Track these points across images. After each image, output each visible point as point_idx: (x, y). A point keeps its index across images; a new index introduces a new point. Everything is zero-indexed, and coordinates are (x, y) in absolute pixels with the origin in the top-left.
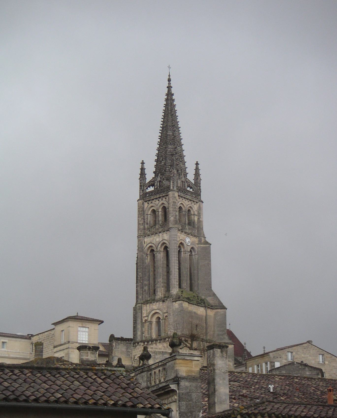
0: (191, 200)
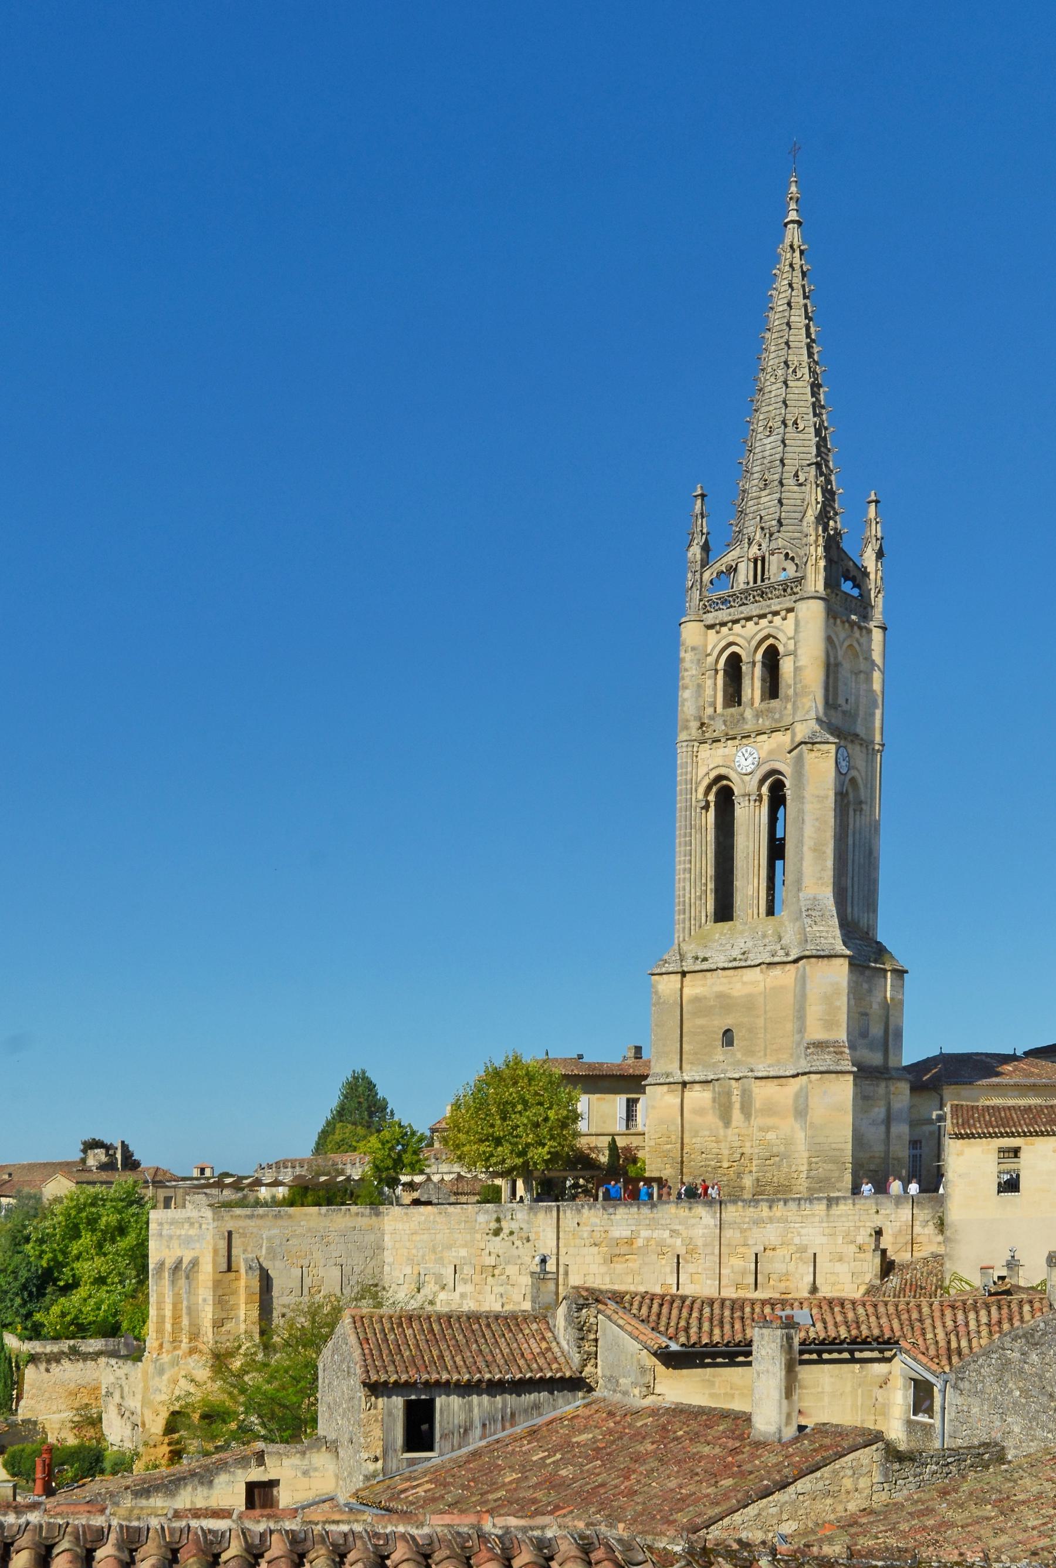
0: (762, 616)
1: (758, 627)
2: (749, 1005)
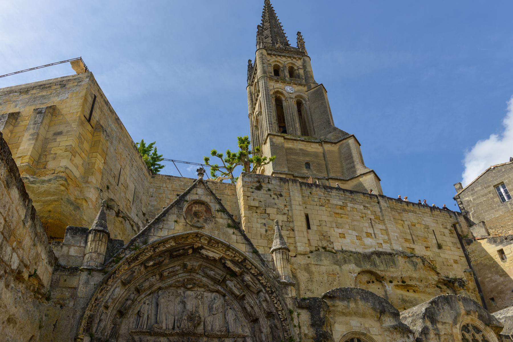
2: (316, 155)
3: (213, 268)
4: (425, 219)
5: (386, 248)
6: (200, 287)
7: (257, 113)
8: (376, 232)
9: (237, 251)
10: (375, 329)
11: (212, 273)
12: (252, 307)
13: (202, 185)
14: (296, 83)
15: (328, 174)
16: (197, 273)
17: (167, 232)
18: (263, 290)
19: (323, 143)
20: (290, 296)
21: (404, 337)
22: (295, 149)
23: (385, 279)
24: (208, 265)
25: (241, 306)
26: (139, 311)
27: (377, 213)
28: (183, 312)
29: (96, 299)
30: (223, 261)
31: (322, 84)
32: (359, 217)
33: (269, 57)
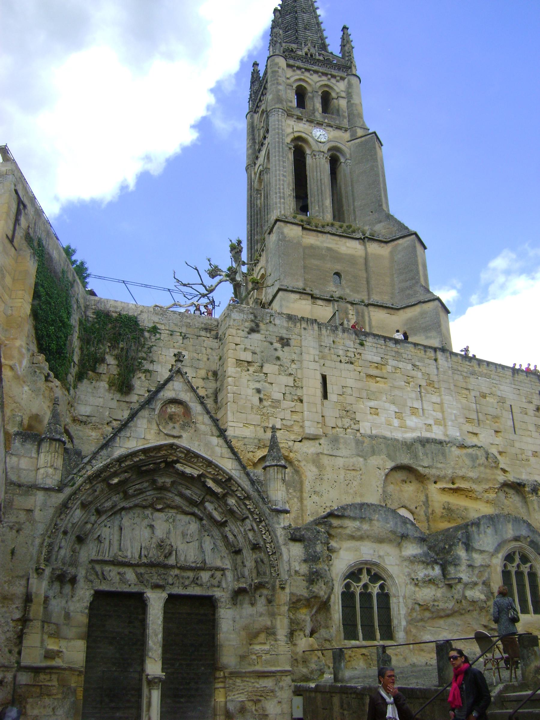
1: (320, 79)
2: (351, 260)
3: (190, 485)
4: (502, 388)
5: (437, 433)
6: (172, 508)
7: (261, 168)
8: (425, 407)
9: (221, 469)
10: (391, 558)
11: (188, 492)
12: (235, 536)
13: (180, 376)
14: (332, 123)
15: (369, 295)
16: (170, 491)
17: (135, 442)
18: (250, 517)
19: (366, 239)
20: (282, 525)
21: (426, 569)
22: (318, 248)
23: (428, 479)
24: (183, 482)
25: (222, 534)
26: (99, 536)
27: (431, 376)
28: (152, 538)
29: (56, 525)
30: (203, 479)
31: (375, 133)
32: (403, 383)
33: (289, 73)
